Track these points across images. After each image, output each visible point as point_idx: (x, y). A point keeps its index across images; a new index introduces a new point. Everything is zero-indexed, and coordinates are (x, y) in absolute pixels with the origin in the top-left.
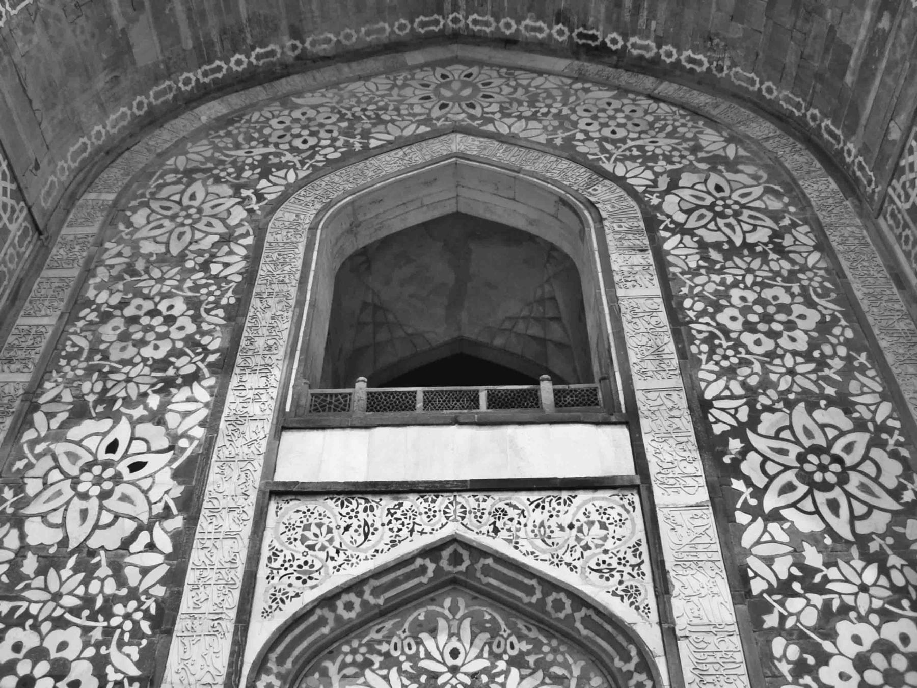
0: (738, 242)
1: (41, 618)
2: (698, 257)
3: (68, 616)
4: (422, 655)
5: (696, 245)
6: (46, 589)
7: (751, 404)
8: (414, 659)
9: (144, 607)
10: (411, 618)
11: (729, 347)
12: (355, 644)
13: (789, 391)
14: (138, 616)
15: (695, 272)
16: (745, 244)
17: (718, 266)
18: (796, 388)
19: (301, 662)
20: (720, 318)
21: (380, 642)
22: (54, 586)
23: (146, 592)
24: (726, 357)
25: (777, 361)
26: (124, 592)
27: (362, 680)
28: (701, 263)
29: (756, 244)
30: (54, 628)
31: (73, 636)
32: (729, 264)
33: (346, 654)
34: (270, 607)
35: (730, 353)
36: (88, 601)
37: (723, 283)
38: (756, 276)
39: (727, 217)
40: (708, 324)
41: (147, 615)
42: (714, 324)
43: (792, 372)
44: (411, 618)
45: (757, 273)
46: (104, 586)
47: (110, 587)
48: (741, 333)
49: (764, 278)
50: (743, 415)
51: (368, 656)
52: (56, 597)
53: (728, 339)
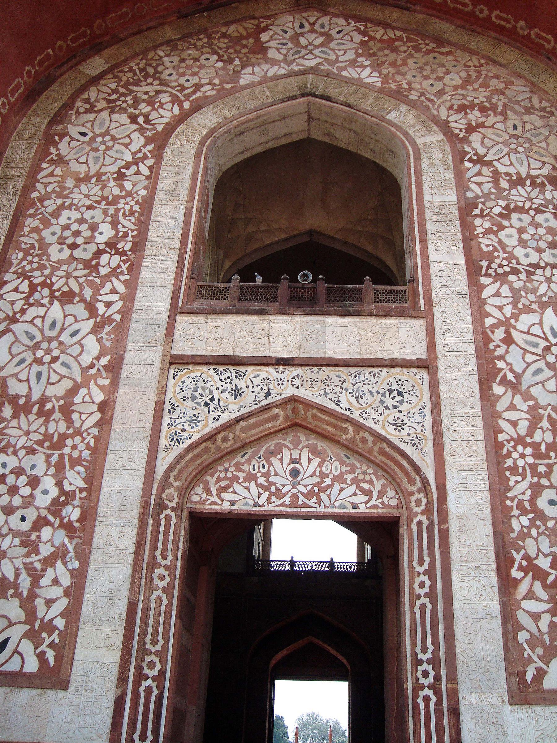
0: (524, 175)
1: (18, 447)
2: (491, 185)
3: (35, 446)
4: (272, 472)
5: (491, 175)
6: (20, 428)
7: (515, 304)
8: (267, 475)
9: (86, 441)
10: (264, 449)
11: (504, 259)
12: (226, 465)
13: (544, 295)
14: (82, 447)
15: (486, 196)
16: (529, 176)
17: (505, 193)
18: (550, 294)
19: (192, 476)
20: (501, 235)
21: (243, 464)
22: (25, 427)
23: (86, 431)
24: (501, 266)
25: (539, 271)
26: (71, 431)
27: (231, 489)
28: (493, 190)
29: (537, 176)
30: (27, 454)
31: (40, 460)
32: (514, 192)
33: (221, 472)
34: (170, 445)
35: (505, 263)
36: (48, 436)
37: (507, 207)
38: (532, 203)
39: (517, 152)
40: (491, 239)
41: (88, 447)
42: (497, 240)
43: (548, 280)
44: (264, 449)
45: (534, 201)
46: (58, 426)
47: (62, 427)
48: (515, 247)
49: (539, 205)
50: (508, 311)
51: (235, 473)
52: (27, 433)
53: (505, 252)
